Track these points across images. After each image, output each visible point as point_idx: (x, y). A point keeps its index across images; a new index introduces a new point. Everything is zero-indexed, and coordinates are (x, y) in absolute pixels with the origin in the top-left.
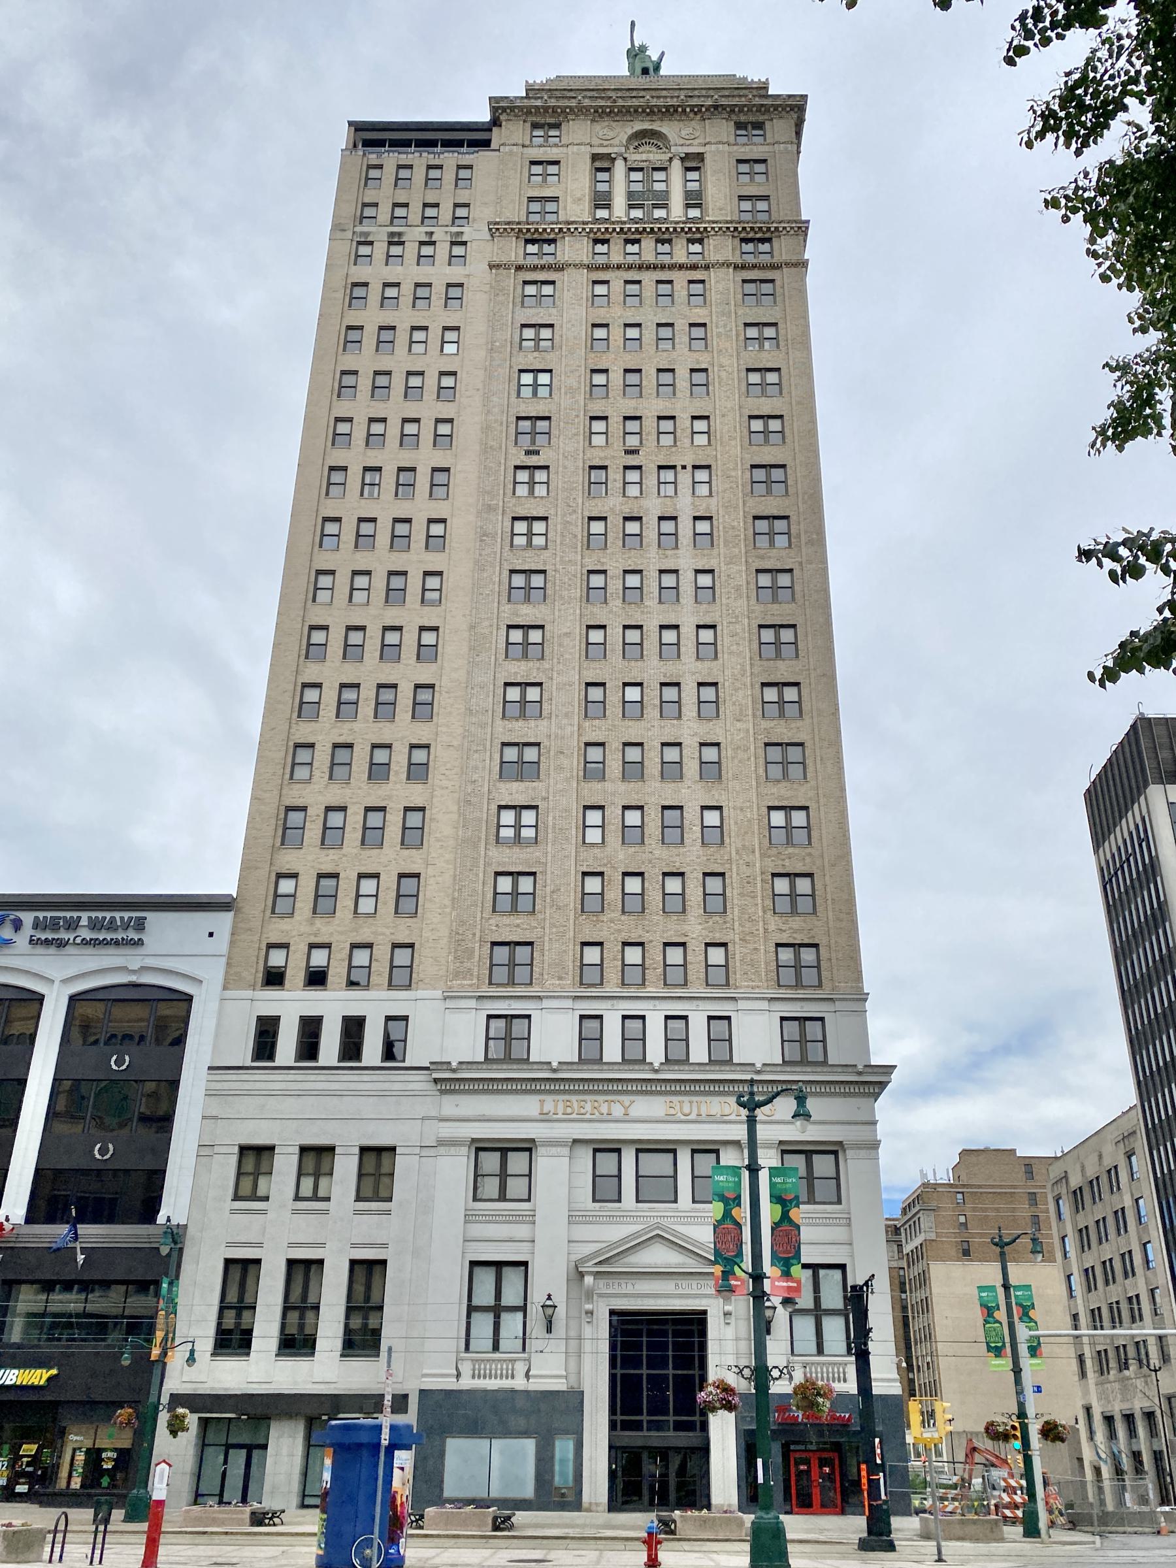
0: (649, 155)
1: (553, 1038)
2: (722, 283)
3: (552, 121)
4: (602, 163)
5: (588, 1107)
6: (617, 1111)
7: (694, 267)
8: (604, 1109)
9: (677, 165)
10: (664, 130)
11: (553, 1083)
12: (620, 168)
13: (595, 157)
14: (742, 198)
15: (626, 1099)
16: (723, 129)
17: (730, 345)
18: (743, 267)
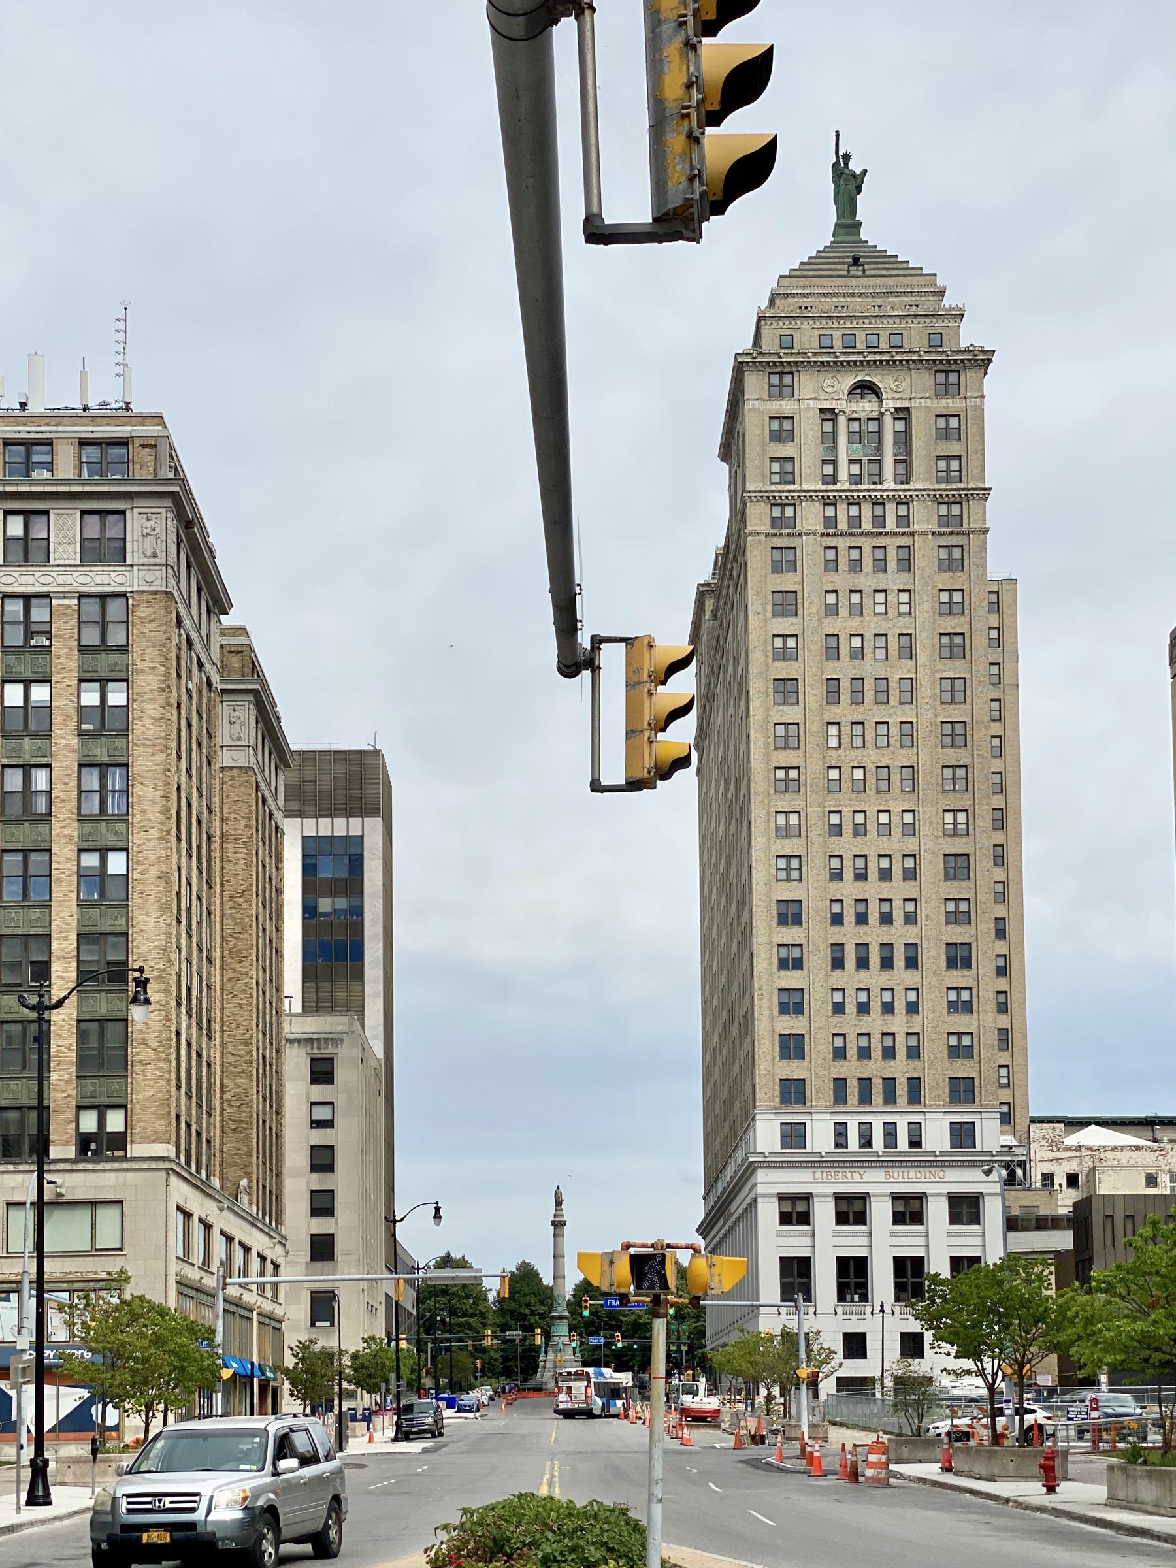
0: (867, 406)
1: (820, 1137)
2: (925, 553)
3: (787, 370)
4: (829, 415)
5: (840, 1175)
6: (857, 1177)
7: (903, 534)
8: (849, 1175)
10: (875, 380)
11: (819, 1163)
12: (842, 420)
13: (821, 410)
14: (939, 458)
15: (862, 1170)
16: (924, 379)
18: (941, 534)
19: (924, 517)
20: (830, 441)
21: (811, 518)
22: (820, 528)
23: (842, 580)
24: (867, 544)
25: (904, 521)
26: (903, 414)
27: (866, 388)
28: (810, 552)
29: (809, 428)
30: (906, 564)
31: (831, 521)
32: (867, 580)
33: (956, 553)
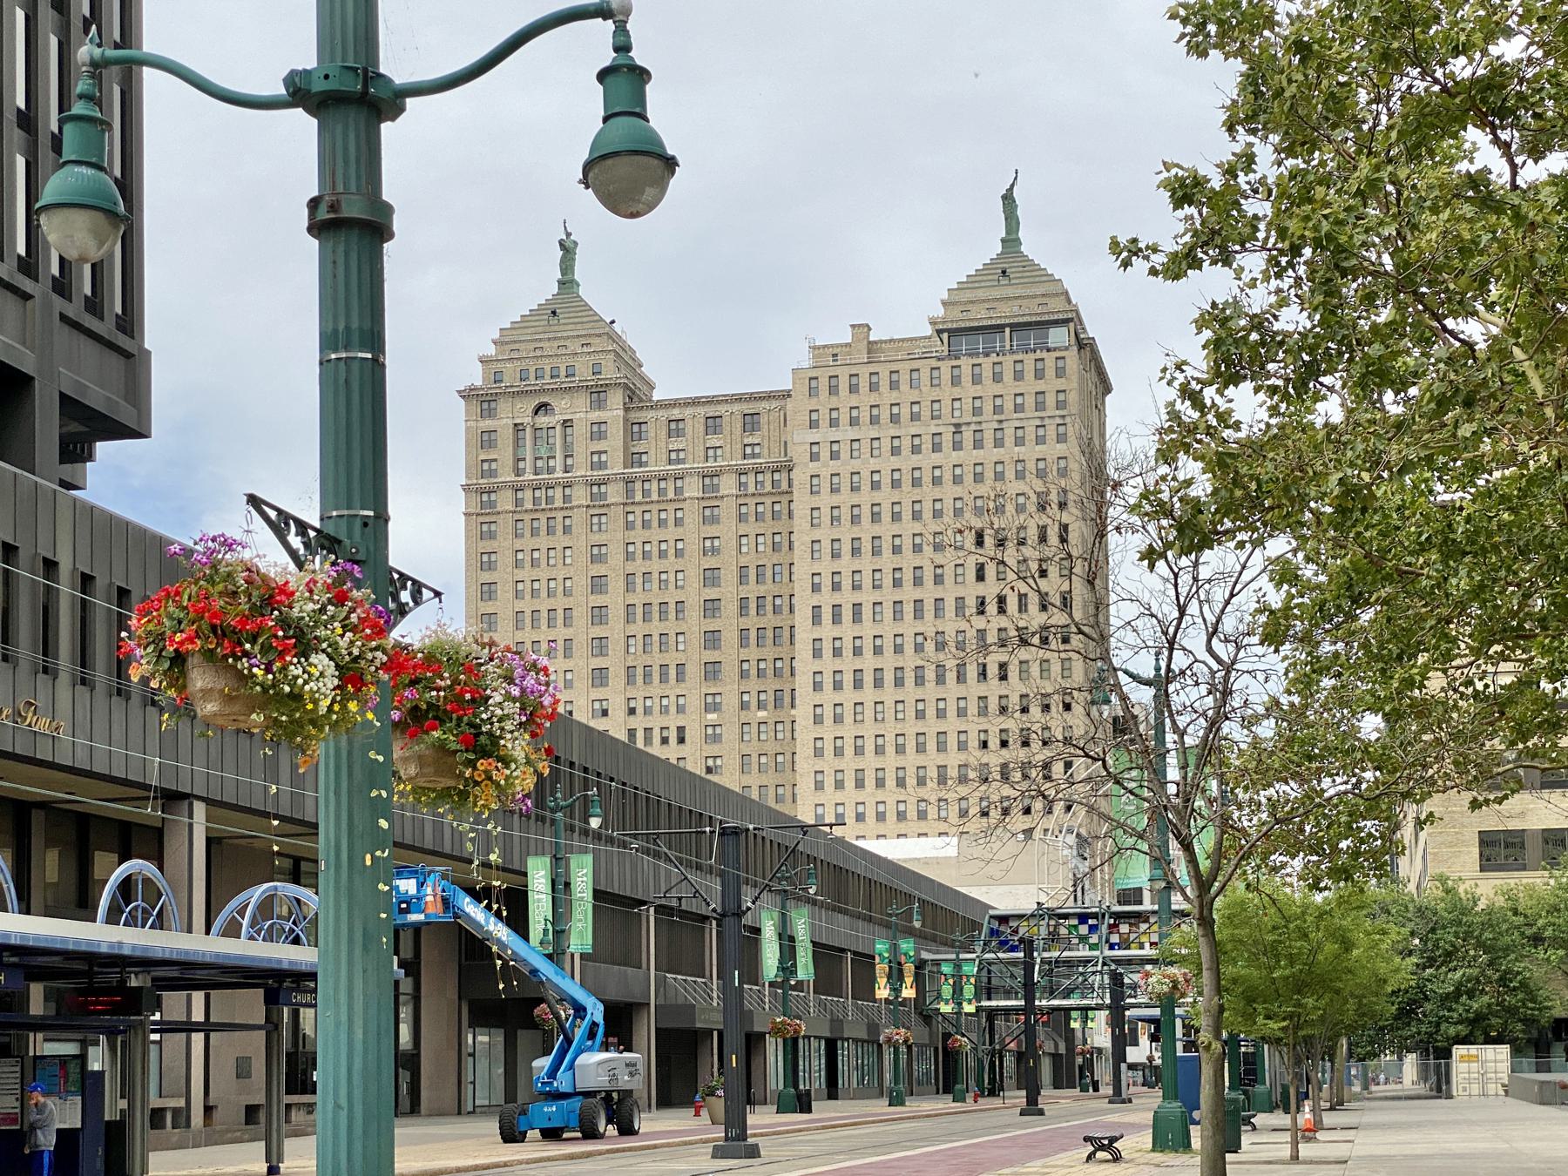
0: (543, 420)
9: (558, 427)
12: (528, 430)
16: (582, 400)
17: (584, 559)
19: (580, 496)
20: (518, 443)
21: (505, 501)
22: (512, 509)
23: (527, 542)
24: (543, 517)
25: (566, 499)
26: (567, 424)
27: (542, 408)
28: (504, 525)
29: (505, 437)
30: (567, 530)
31: (518, 502)
32: (543, 542)
33: (604, 519)
